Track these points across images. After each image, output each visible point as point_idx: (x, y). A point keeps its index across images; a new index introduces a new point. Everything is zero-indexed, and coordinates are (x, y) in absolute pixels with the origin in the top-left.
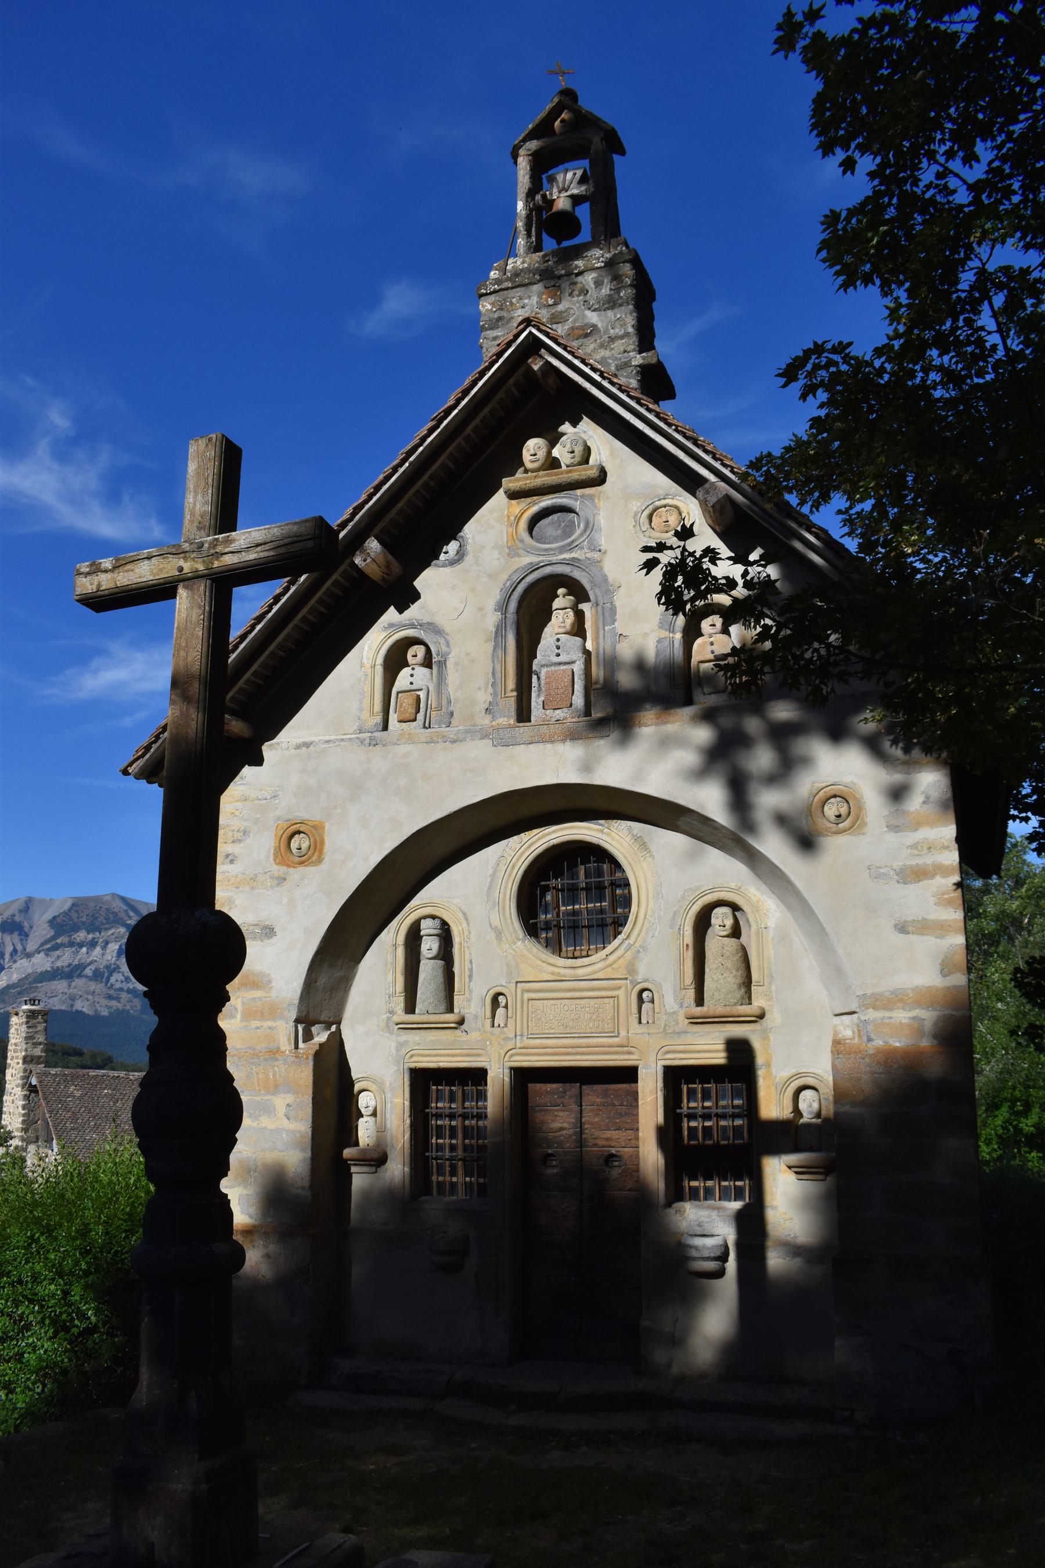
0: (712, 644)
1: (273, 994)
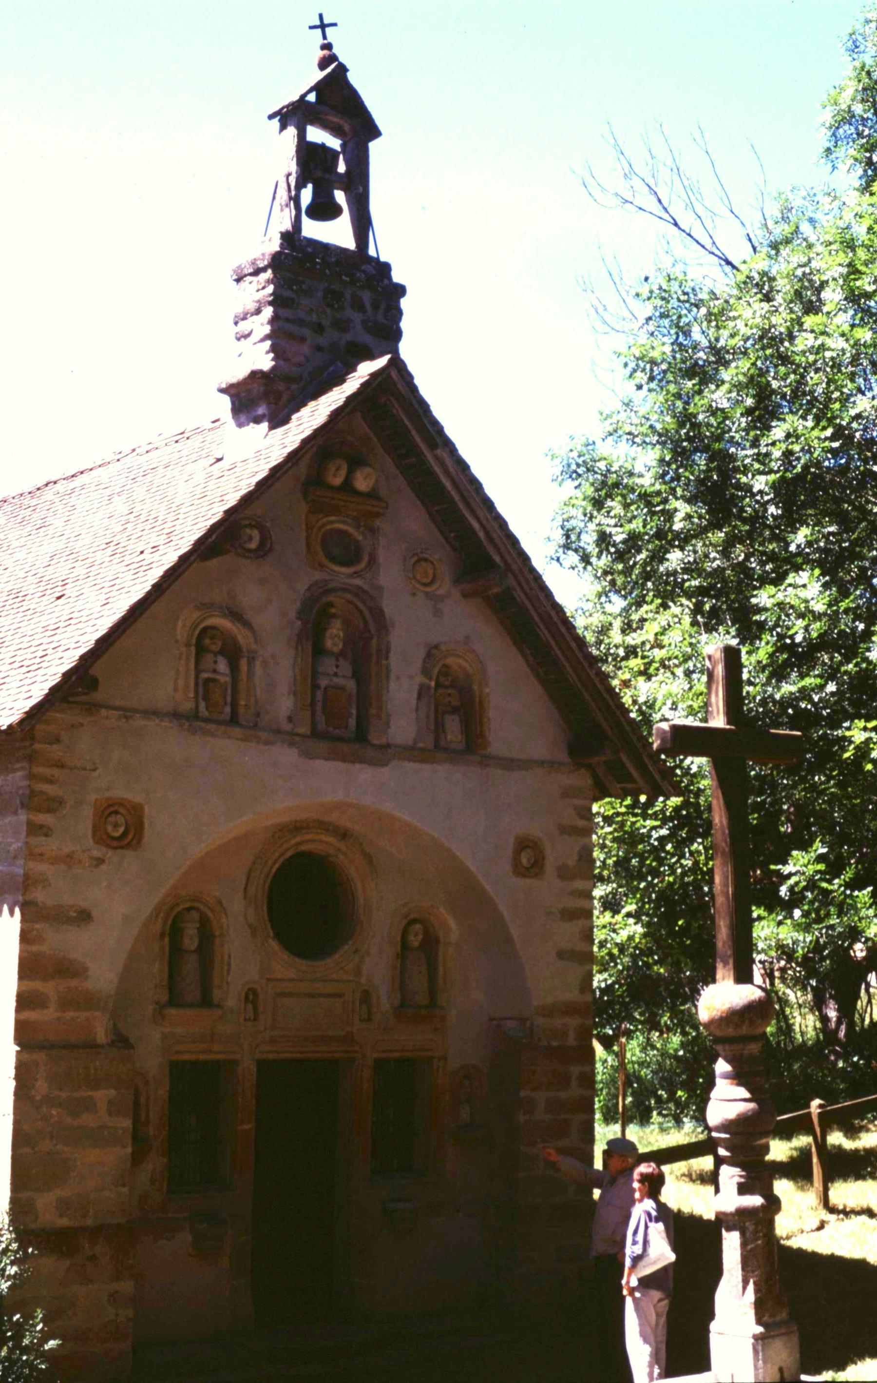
0: (449, 695)
1: (89, 985)
